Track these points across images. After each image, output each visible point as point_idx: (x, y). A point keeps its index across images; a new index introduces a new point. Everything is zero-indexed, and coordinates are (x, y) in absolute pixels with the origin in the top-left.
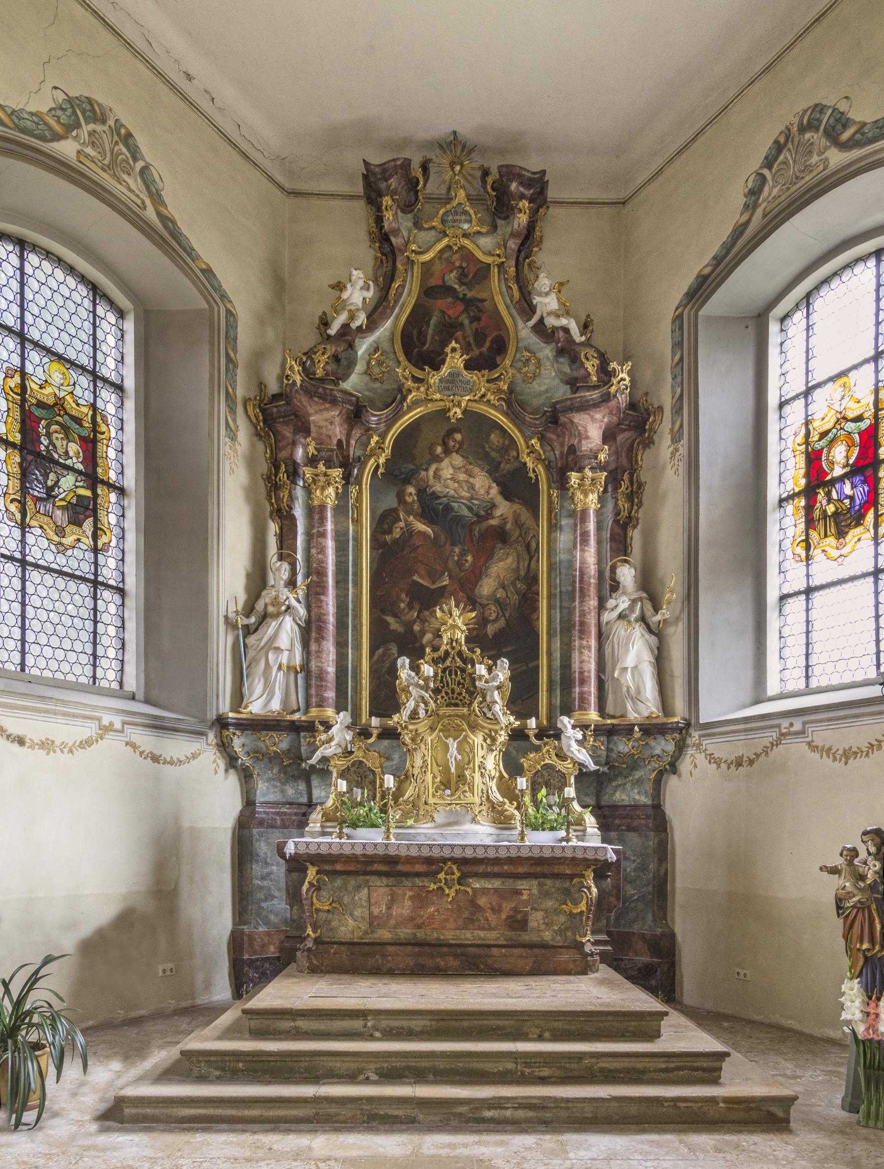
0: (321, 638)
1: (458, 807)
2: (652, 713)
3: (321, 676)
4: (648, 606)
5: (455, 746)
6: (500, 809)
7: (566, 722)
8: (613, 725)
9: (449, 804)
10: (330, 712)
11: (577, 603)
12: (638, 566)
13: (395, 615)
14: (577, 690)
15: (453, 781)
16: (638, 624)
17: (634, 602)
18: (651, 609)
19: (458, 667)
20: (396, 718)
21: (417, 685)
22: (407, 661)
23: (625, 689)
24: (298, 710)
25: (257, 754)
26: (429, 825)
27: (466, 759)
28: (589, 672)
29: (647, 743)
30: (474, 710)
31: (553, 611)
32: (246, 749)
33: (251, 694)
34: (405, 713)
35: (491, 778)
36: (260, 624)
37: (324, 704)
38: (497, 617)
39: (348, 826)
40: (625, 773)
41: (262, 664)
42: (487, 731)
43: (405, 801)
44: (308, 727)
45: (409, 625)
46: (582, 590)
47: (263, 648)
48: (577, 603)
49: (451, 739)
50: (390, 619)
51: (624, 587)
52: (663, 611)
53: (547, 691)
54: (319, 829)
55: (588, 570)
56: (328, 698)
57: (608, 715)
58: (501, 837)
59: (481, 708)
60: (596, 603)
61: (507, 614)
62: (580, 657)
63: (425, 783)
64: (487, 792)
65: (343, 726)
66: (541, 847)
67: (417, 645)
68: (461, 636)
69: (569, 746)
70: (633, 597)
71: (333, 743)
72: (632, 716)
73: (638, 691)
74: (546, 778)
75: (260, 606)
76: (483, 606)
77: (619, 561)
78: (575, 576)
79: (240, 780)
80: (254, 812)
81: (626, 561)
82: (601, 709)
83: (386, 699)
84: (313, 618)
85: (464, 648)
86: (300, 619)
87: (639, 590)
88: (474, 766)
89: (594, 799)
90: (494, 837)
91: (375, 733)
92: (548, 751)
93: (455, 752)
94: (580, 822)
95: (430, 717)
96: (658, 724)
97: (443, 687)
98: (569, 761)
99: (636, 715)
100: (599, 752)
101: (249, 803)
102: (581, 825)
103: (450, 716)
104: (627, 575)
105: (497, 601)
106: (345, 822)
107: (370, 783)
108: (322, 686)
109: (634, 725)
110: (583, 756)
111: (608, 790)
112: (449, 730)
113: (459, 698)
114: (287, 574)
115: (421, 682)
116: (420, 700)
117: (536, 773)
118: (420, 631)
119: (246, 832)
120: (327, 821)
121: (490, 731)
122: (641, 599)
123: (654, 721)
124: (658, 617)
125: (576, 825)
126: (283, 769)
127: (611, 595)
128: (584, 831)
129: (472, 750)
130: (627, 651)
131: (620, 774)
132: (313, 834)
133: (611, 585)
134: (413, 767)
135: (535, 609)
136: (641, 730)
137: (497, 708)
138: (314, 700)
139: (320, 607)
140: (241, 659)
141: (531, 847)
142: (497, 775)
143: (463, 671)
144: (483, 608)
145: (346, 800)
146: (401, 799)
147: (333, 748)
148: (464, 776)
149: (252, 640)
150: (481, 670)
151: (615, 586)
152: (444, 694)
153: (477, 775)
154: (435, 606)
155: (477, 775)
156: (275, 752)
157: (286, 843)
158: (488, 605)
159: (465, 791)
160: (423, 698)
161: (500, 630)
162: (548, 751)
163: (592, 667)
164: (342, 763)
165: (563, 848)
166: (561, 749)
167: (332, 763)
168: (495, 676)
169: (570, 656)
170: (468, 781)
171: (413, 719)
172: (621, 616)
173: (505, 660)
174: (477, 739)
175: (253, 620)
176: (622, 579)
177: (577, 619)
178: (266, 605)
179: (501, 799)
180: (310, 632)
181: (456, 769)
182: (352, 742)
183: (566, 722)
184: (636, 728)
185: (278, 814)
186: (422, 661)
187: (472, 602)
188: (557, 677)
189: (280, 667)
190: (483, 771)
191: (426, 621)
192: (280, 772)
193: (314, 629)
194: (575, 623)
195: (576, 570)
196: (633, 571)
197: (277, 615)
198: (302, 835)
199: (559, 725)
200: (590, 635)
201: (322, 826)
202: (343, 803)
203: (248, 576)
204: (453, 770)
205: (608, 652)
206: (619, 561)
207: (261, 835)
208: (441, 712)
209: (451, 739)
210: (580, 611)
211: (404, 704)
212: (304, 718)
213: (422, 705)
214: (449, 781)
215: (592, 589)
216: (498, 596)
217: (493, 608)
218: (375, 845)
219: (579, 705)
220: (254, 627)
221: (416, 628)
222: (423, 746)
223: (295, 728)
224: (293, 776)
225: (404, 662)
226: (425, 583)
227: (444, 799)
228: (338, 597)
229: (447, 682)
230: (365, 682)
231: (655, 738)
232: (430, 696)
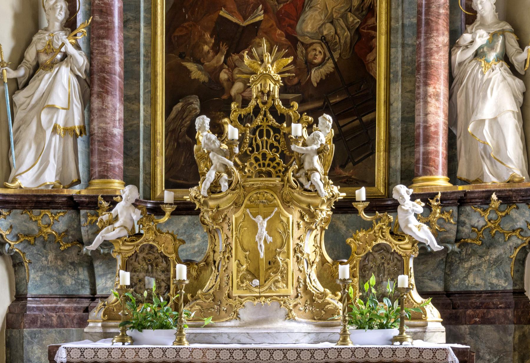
0: (104, 92)
1: (268, 301)
2: (514, 176)
3: (106, 140)
4: (512, 40)
5: (265, 225)
6: (320, 301)
7: (402, 191)
8: (465, 193)
9: (258, 297)
10: (116, 184)
11: (422, 40)
13: (197, 61)
14: (421, 149)
15: (264, 269)
16: (499, 64)
17: (494, 36)
19: (271, 126)
20: (193, 191)
21: (220, 151)
22: (207, 121)
23: (481, 147)
24: (79, 182)
25: (27, 237)
26: (232, 323)
27: (279, 241)
28: (437, 126)
29: (507, 214)
30: (288, 181)
31: (393, 50)
32: (15, 232)
33: (20, 165)
34: (205, 186)
35: (310, 264)
36: (31, 77)
37: (110, 174)
38: (323, 59)
39: (133, 327)
40: (480, 251)
41: (34, 127)
42: (304, 206)
43: (204, 294)
44: (89, 203)
45: (214, 73)
47: (34, 107)
48: (422, 40)
49: (260, 218)
50: (191, 66)
51: (482, 17)
53: (385, 151)
54: (100, 330)
56: (114, 167)
57: (460, 179)
58: (321, 337)
59: (297, 178)
61: (336, 56)
63: (229, 271)
64: (305, 281)
65: (129, 203)
66: (367, 350)
67: (225, 97)
68: (274, 88)
69: (407, 221)
70: (492, 31)
71: (117, 224)
72: (491, 181)
73: (498, 150)
74: (379, 262)
75: (30, 55)
76: (306, 46)
79: (8, 269)
80: (25, 308)
83: (184, 169)
84: (95, 69)
85: (279, 103)
86: (79, 70)
88: (288, 249)
89: (442, 283)
90: (312, 336)
91: (168, 210)
92: (381, 228)
93: (265, 233)
94: (419, 315)
95: (234, 190)
96: (521, 190)
97: (252, 152)
98: (407, 240)
99: (494, 180)
100: (447, 227)
101: (19, 297)
102: (420, 319)
103: (259, 188)
105: (324, 40)
106: (128, 322)
107: (163, 272)
108: (106, 152)
109: (491, 192)
110: (424, 234)
111: (459, 273)
112: (257, 206)
113: (272, 164)
114: (63, 13)
115: (225, 147)
116: (222, 169)
117: (367, 255)
118: (228, 80)
119: (15, 332)
120: (109, 319)
121: (309, 206)
122: (503, 32)
123: (517, 187)
124: (524, 55)
125: (413, 319)
126: (61, 256)
128: (425, 326)
129: (286, 231)
131: (474, 252)
132: (94, 337)
134: (214, 252)
135: (372, 48)
136: (499, 198)
137: (317, 177)
138: (97, 169)
139: (104, 54)
140: (7, 122)
141: (353, 350)
142: (317, 260)
143: (277, 130)
144: (306, 49)
145: (131, 296)
146: (199, 292)
147: (117, 230)
148: (275, 262)
149: (20, 97)
150: (298, 129)
152: (253, 161)
153: (292, 261)
154: (245, 48)
155: (292, 261)
156: (50, 235)
157: (58, 347)
158: (312, 44)
159: (277, 281)
160: (225, 166)
161: (327, 75)
162: (381, 228)
164: (128, 249)
165: (394, 350)
166: (397, 225)
167: (116, 248)
168: (316, 137)
170: (281, 268)
171: (213, 193)
172: (477, 55)
173: (328, 117)
174: (293, 216)
175: (22, 72)
176: (480, 7)
177: (422, 60)
178: (38, 53)
179: (322, 289)
180: (92, 85)
181: (266, 254)
182: (140, 222)
183: (402, 191)
184: (494, 196)
185: (54, 309)
186: (226, 120)
187: (292, 43)
188: (397, 133)
189: (55, 130)
190: (299, 255)
191: (236, 66)
192: (56, 258)
193: (96, 81)
197: (50, 66)
198: (81, 338)
199: (395, 196)
201: (103, 326)
202: (127, 299)
203: (17, 17)
204: (262, 255)
205: (460, 100)
207: (33, 335)
208: (248, 184)
209: (260, 218)
210: (426, 49)
211: (204, 174)
212: (84, 193)
213: (225, 176)
214: (258, 269)
215: (441, 21)
216: (325, 33)
217: (319, 48)
218: (164, 351)
219: (424, 169)
220: (24, 81)
221: (224, 76)
222: (225, 226)
223: (73, 204)
224: (72, 263)
225: (203, 122)
226: (234, 20)
227: (251, 291)
228: (126, 39)
229: (257, 145)
230: (161, 145)
231: (518, 208)
232: (236, 164)
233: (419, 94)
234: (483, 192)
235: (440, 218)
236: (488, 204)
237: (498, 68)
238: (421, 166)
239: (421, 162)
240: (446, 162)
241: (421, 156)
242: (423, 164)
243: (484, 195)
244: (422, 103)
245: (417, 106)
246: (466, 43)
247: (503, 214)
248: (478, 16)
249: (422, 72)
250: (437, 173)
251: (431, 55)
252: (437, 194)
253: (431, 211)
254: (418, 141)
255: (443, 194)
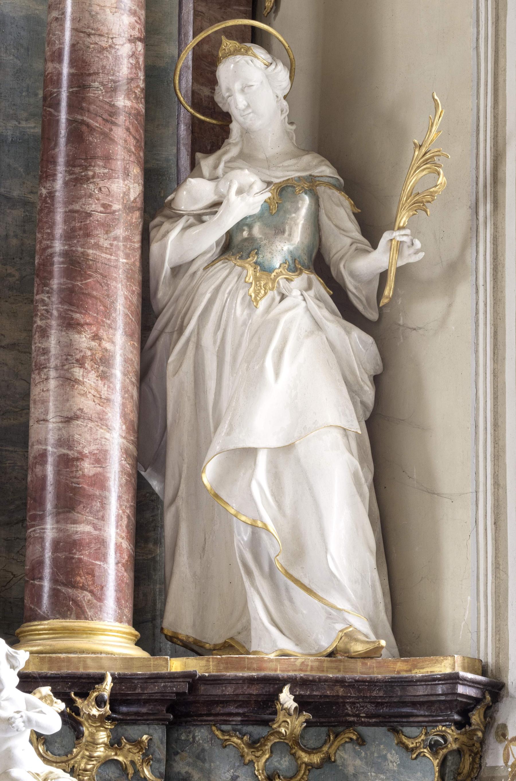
2: (350, 636)
4: (340, 214)
8: (192, 680)
11: (59, 184)
12: (302, 62)
14: (50, 530)
16: (299, 281)
17: (283, 193)
18: (352, 227)
23: (243, 536)
28: (100, 459)
29: (327, 760)
46: (78, 134)
48: (59, 184)
51: (246, 132)
52: (397, 235)
55: (108, 61)
57: (173, 638)
60: (135, 190)
62: (65, 399)
70: (279, 176)
72: (276, 644)
73: (298, 551)
77: (229, 33)
78: (54, 80)
81: (256, 37)
82: (146, 618)
87: (307, 151)
96: (372, 683)
99: (287, 645)
104: (256, 87)
109: (276, 684)
122: (311, 185)
123: (359, 671)
124: (378, 260)
127: (194, 165)
130: (255, 381)
133: (195, 125)
136: (303, 704)
151: (213, 129)
163: (110, 440)
169: (27, 395)
172: (231, 246)
177: (58, 246)
184: (286, 698)
194: (47, 262)
195: (58, 57)
196: (281, 74)
200: (107, 313)
205: (177, 381)
206: (229, 33)
210: (70, 215)
215: (119, 133)
219: (55, 594)
231: (361, 741)
233: (45, 352)
234: (251, 681)
235: (108, 762)
236: (266, 723)
237: (296, 293)
238: (46, 585)
239: (47, 572)
240: (128, 577)
241: (48, 555)
242: (54, 580)
243: (254, 690)
244: (52, 384)
245: (36, 392)
246: (197, 207)
247: (316, 759)
248: (234, 127)
249: (55, 283)
250: (97, 616)
251: (88, 235)
252: (101, 679)
253: (79, 735)
254: (40, 502)
255: (117, 680)
